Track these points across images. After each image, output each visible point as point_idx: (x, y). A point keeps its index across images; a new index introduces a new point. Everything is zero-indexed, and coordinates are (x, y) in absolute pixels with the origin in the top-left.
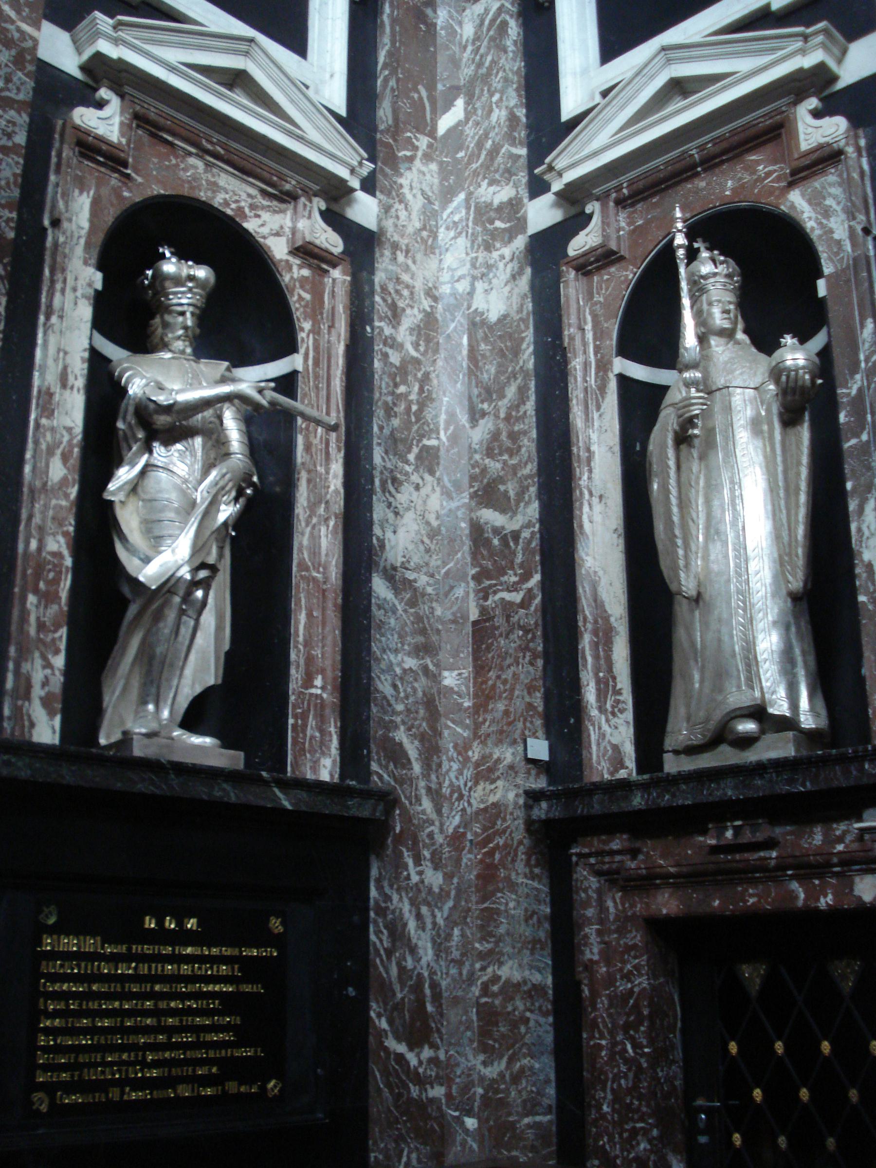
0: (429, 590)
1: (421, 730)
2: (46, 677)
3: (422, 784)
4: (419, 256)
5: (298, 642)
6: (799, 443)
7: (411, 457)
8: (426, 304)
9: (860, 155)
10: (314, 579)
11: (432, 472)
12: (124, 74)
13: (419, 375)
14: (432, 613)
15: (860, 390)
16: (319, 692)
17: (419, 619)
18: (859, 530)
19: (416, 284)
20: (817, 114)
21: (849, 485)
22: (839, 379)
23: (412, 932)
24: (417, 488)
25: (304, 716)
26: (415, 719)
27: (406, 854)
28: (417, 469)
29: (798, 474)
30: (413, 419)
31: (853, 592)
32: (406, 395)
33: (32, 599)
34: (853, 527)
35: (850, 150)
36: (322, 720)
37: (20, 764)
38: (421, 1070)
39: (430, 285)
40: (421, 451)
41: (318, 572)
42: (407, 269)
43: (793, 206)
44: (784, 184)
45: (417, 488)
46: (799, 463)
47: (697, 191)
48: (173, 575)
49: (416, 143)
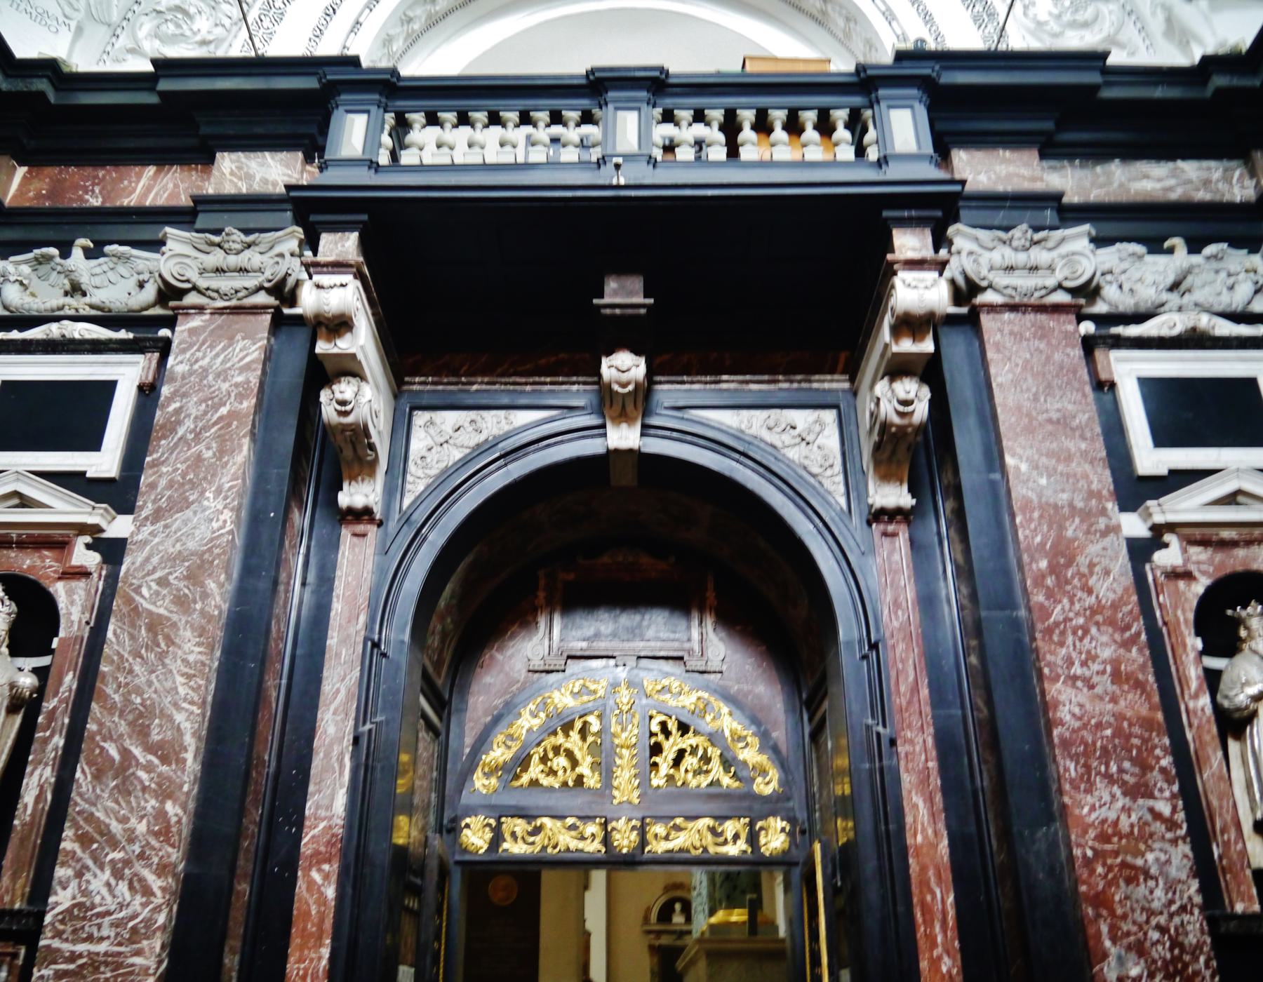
6: (12, 725)
9: (100, 579)
15: (54, 707)
18: (27, 784)
20: (88, 546)
21: (31, 758)
22: (46, 697)
29: (6, 743)
31: (13, 817)
34: (25, 781)
35: (95, 575)
43: (56, 591)
44: (56, 576)
46: (9, 737)
47: (9, 557)
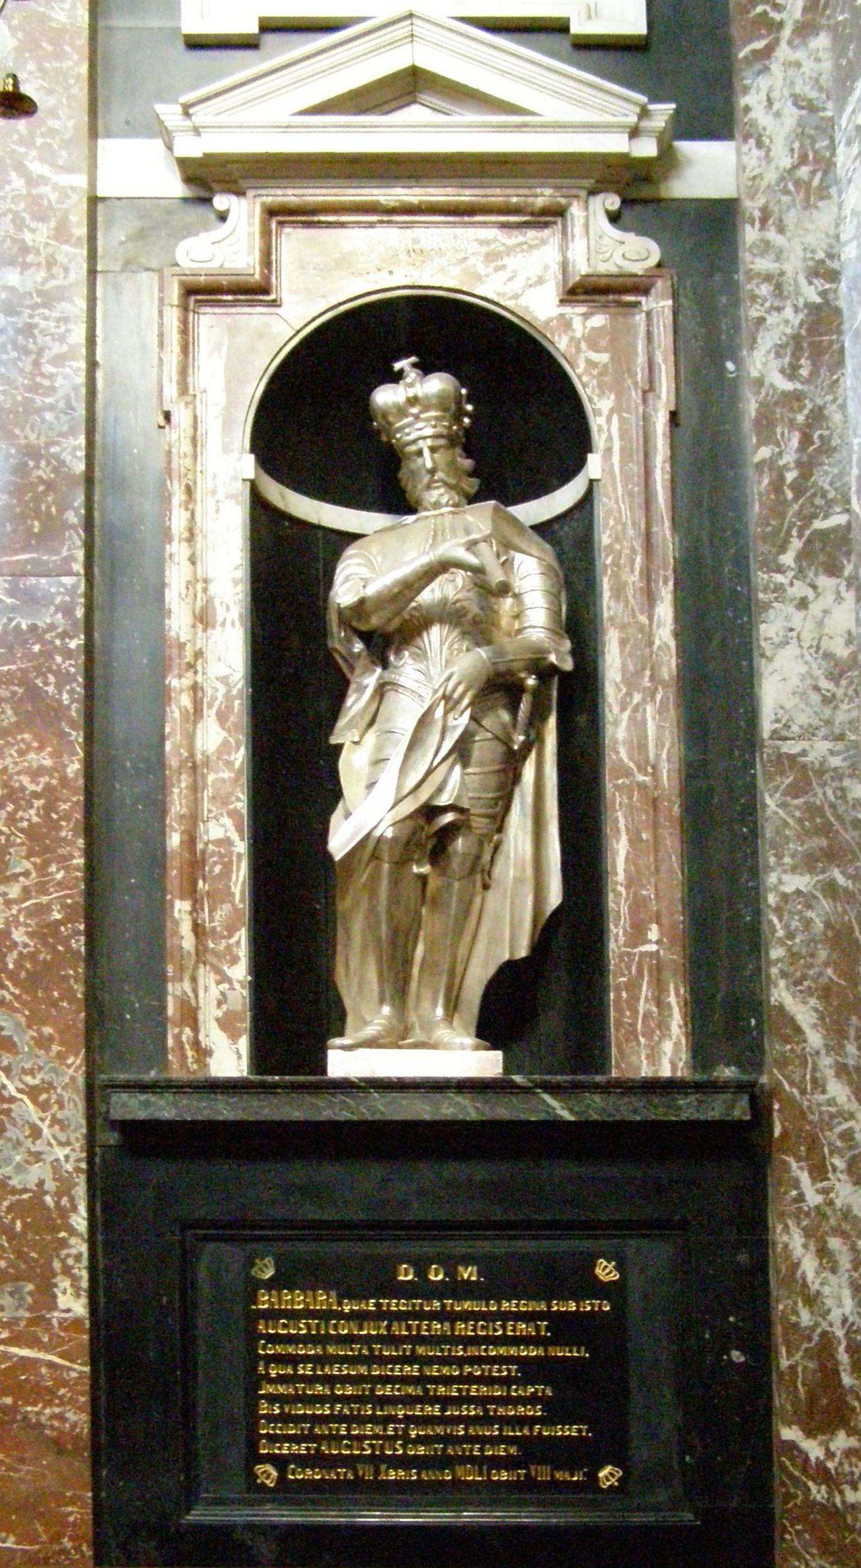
0: (835, 761)
1: (823, 980)
2: (223, 994)
3: (826, 1062)
4: (790, 218)
5: (616, 883)
7: (788, 559)
8: (811, 294)
10: (642, 787)
11: (833, 570)
12: (230, 166)
13: (800, 418)
14: (844, 797)
16: (653, 948)
17: (813, 811)
19: (788, 268)
23: (810, 1275)
24: (803, 604)
25: (633, 987)
26: (811, 966)
27: (794, 1165)
28: (801, 573)
30: (790, 495)
32: (770, 463)
33: (181, 907)
36: (659, 987)
37: (162, 1103)
38: (830, 1465)
39: (820, 255)
40: (809, 541)
41: (646, 774)
42: (766, 247)
45: (803, 604)
48: (368, 836)
49: (776, 16)
